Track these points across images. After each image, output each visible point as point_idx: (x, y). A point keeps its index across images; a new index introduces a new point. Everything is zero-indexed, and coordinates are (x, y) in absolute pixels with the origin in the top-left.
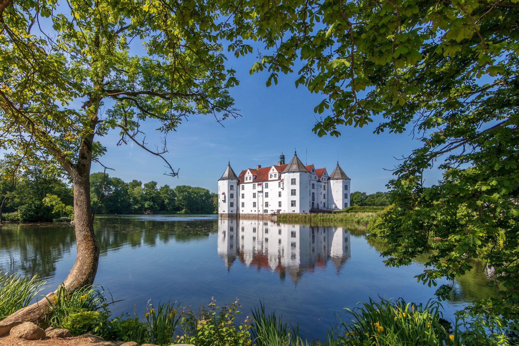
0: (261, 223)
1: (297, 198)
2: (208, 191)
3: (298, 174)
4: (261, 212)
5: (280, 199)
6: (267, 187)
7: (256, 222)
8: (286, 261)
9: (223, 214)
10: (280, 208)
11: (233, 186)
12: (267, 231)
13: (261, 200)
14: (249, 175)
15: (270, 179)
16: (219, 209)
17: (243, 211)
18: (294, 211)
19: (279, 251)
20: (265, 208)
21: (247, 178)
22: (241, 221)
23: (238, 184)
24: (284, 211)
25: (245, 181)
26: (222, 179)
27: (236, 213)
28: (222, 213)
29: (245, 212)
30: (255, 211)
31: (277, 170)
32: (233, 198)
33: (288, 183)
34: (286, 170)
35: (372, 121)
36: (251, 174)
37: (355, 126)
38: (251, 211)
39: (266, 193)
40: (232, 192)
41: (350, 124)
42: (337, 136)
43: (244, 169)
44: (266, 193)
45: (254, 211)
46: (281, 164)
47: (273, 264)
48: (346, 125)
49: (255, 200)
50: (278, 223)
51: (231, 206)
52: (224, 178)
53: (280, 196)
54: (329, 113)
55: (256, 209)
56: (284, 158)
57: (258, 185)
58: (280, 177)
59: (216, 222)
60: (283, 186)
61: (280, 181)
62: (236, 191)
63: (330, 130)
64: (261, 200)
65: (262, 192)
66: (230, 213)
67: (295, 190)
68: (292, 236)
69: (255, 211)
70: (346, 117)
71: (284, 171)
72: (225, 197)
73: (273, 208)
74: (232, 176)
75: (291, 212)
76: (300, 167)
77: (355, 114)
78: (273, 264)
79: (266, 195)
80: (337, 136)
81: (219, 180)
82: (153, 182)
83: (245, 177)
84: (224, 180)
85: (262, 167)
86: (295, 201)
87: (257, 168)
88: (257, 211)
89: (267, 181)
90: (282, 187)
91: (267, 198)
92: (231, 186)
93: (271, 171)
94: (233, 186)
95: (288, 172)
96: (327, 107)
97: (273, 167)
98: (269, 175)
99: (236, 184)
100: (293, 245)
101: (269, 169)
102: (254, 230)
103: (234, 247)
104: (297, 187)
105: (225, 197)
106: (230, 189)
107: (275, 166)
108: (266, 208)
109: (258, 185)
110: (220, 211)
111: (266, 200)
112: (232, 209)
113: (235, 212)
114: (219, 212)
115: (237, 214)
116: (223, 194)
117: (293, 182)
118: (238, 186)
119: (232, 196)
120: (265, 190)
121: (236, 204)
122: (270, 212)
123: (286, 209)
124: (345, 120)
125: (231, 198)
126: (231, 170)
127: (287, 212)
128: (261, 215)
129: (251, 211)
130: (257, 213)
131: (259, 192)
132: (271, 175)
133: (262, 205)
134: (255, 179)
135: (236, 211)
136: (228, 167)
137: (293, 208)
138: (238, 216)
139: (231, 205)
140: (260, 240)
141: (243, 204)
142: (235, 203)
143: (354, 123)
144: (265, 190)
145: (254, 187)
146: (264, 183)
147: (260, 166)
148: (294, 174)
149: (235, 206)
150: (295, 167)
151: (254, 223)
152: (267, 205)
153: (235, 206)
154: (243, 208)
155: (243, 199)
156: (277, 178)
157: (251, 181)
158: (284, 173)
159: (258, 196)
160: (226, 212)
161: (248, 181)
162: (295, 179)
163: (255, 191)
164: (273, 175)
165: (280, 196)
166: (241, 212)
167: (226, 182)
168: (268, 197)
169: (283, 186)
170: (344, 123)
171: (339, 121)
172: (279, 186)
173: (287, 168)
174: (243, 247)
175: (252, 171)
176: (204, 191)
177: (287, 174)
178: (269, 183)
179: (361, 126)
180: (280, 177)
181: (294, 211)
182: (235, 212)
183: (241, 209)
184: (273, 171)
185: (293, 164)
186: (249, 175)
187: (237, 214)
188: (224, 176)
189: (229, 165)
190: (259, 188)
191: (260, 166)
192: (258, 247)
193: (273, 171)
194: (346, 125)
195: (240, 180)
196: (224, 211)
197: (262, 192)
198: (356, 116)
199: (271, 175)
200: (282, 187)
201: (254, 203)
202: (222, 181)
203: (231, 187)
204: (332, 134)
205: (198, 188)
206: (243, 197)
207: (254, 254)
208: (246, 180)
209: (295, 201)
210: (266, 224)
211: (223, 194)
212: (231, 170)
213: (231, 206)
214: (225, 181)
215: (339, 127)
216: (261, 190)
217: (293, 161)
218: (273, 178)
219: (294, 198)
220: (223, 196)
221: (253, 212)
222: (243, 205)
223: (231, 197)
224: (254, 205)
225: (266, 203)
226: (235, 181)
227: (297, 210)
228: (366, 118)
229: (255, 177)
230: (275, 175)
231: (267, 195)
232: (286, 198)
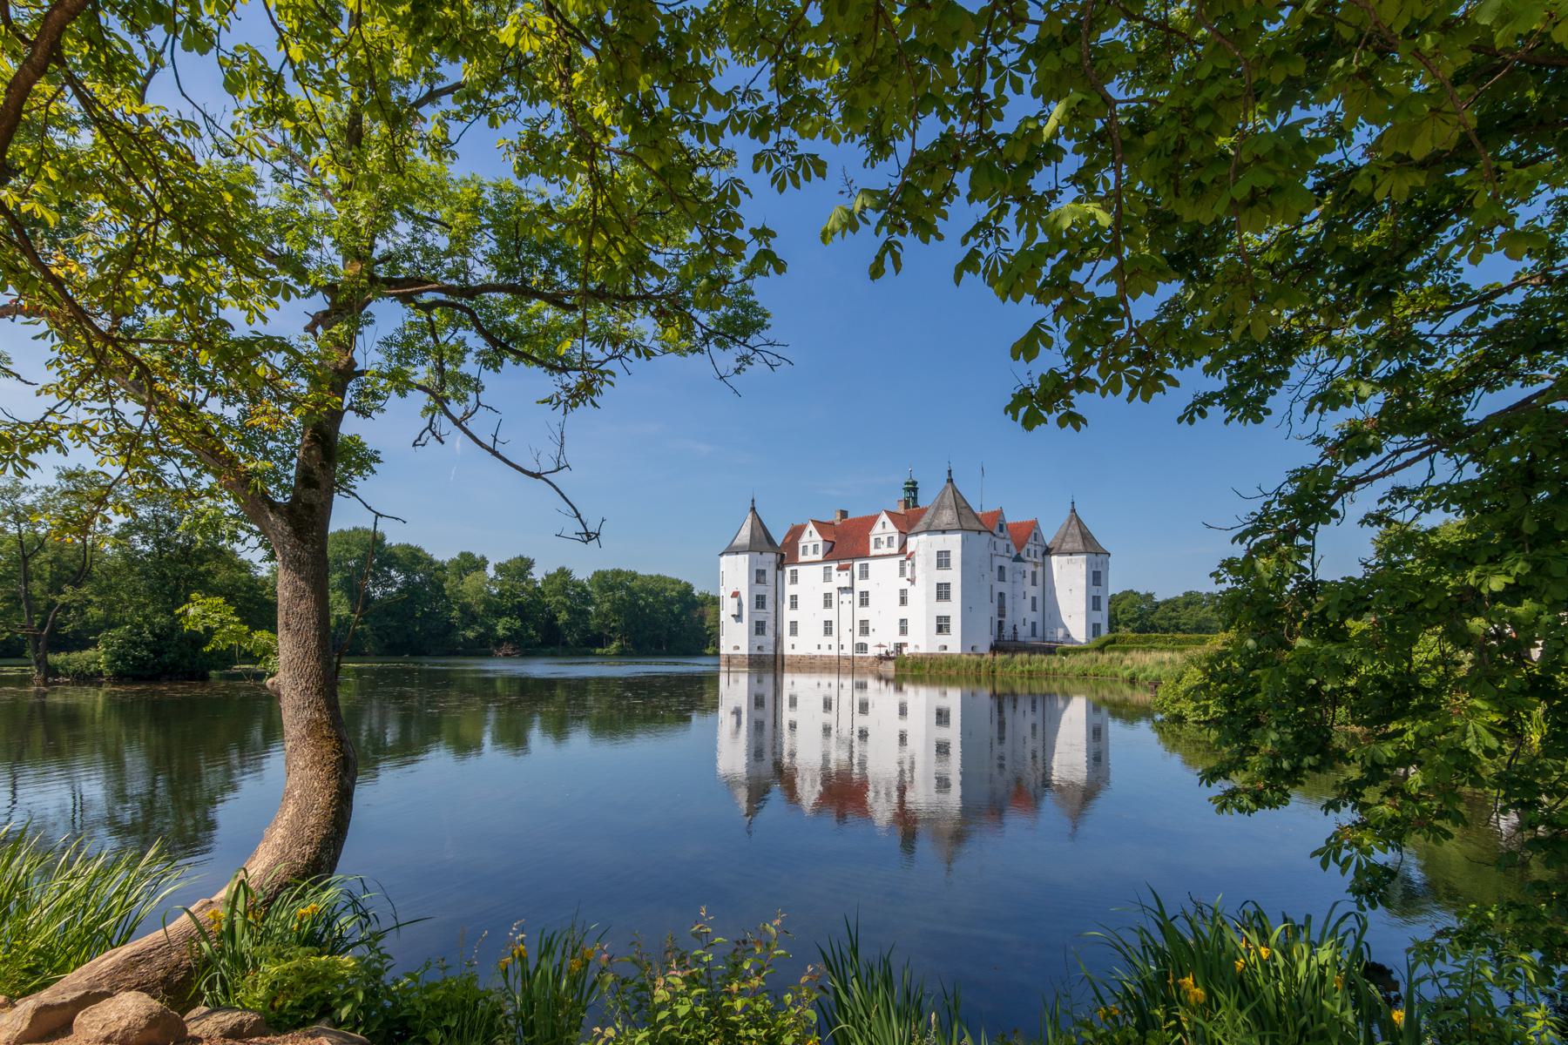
0: (848, 682)
2: (688, 589)
3: (958, 537)
5: (903, 612)
6: (865, 574)
7: (834, 680)
8: (921, 796)
9: (735, 656)
11: (763, 572)
12: (864, 707)
13: (846, 613)
14: (811, 539)
15: (873, 552)
16: (722, 642)
17: (793, 646)
18: (945, 648)
19: (902, 772)
20: (860, 639)
21: (805, 547)
22: (788, 678)
23: (780, 566)
24: (917, 647)
25: (801, 558)
26: (733, 550)
27: (772, 653)
28: (732, 652)
29: (798, 652)
30: (830, 647)
31: (896, 526)
32: (763, 607)
33: (928, 563)
34: (921, 525)
35: (1176, 384)
36: (817, 538)
37: (1130, 400)
38: (819, 647)
39: (862, 593)
40: (760, 590)
41: (1116, 391)
42: (1078, 429)
43: (797, 523)
44: (862, 593)
45: (826, 647)
46: (907, 506)
47: (882, 809)
48: (1103, 394)
49: (830, 614)
50: (898, 682)
51: (757, 633)
52: (737, 547)
53: (903, 601)
54: (1053, 359)
55: (832, 640)
56: (915, 490)
57: (839, 569)
58: (903, 545)
59: (714, 679)
60: (913, 572)
61: (903, 558)
62: (773, 588)
63: (1057, 411)
64: (846, 613)
65: (851, 589)
66: (755, 652)
67: (948, 585)
68: (939, 723)
69: (830, 647)
70: (1103, 372)
71: (916, 529)
72: (740, 605)
73: (883, 638)
74: (762, 540)
75: (935, 650)
76: (962, 517)
77: (1129, 363)
78: (882, 809)
79: (862, 601)
80: (1078, 429)
81: (722, 555)
82: (521, 558)
83: (801, 546)
84: (737, 553)
85: (851, 516)
86: (947, 618)
87: (836, 518)
88: (835, 647)
89: (866, 556)
90: (908, 575)
91: (864, 609)
92: (758, 571)
93: (877, 529)
94: (763, 572)
95: (929, 531)
96: (1048, 343)
97: (884, 517)
98: (872, 540)
99: (773, 566)
100: (942, 749)
101: (870, 521)
102: (827, 705)
103: (768, 758)
104: (953, 576)
105: (740, 605)
107: (889, 514)
108: (863, 639)
109: (839, 569)
110: (726, 648)
111: (862, 613)
112: (760, 640)
113: (769, 651)
114: (723, 651)
115: (776, 656)
116: (736, 595)
117: (943, 560)
118: (780, 572)
119: (760, 602)
120: (860, 586)
121: (773, 627)
122: (873, 652)
123: (921, 641)
124: (1100, 381)
125: (757, 607)
126: (759, 524)
127: (923, 650)
128: (846, 658)
129: (819, 647)
130: (834, 652)
131: (842, 590)
132: (877, 540)
133: (852, 630)
134: (831, 550)
135: (772, 647)
136: (750, 515)
137: (943, 639)
138: (779, 662)
139: (759, 628)
140: (845, 733)
141: (794, 625)
142: (770, 624)
143: (1126, 388)
144: (860, 586)
145: (827, 577)
146: (857, 564)
147: (844, 514)
148: (946, 536)
149: (770, 635)
150: (948, 516)
151: (826, 683)
152: (865, 628)
154: (793, 639)
155: (794, 611)
156: (895, 550)
157: (819, 557)
158: (917, 534)
159: (840, 603)
160: (744, 650)
161: (811, 557)
163: (831, 588)
164: (884, 538)
165: (903, 601)
166: (788, 651)
167: (743, 560)
168: (867, 604)
169: (913, 572)
170: (1098, 390)
171: (1083, 384)
172: (902, 572)
173: (926, 519)
174: (792, 755)
175: (821, 526)
176: (678, 588)
177: (923, 537)
178: (872, 563)
179: (1146, 398)
180: (903, 545)
181: (945, 648)
182: (769, 651)
183: (788, 640)
184: (884, 530)
185: (943, 508)
186: (811, 539)
187: (776, 656)
188: (737, 542)
189: (753, 509)
190: (842, 579)
191: (844, 514)
192: (838, 756)
193: (884, 530)
194: (1103, 394)
195: (786, 555)
196: (737, 648)
197: (851, 589)
198: (1133, 367)
199: (877, 540)
200: (908, 575)
201: (826, 622)
202: (733, 557)
203: (759, 576)
204: (1061, 423)
205: (660, 578)
206: (794, 605)
207: (826, 778)
208: (804, 553)
209: (947, 618)
210: (862, 686)
211: (736, 595)
212: (759, 524)
213: (757, 633)
215: (1082, 402)
216: (848, 585)
217: (942, 498)
218: (884, 550)
219: (945, 608)
221: (825, 652)
223: (757, 604)
224: (826, 629)
226: (771, 557)
227: (953, 643)
228: (1161, 375)
229: (830, 545)
230: (890, 539)
231: (864, 600)
232: (922, 609)
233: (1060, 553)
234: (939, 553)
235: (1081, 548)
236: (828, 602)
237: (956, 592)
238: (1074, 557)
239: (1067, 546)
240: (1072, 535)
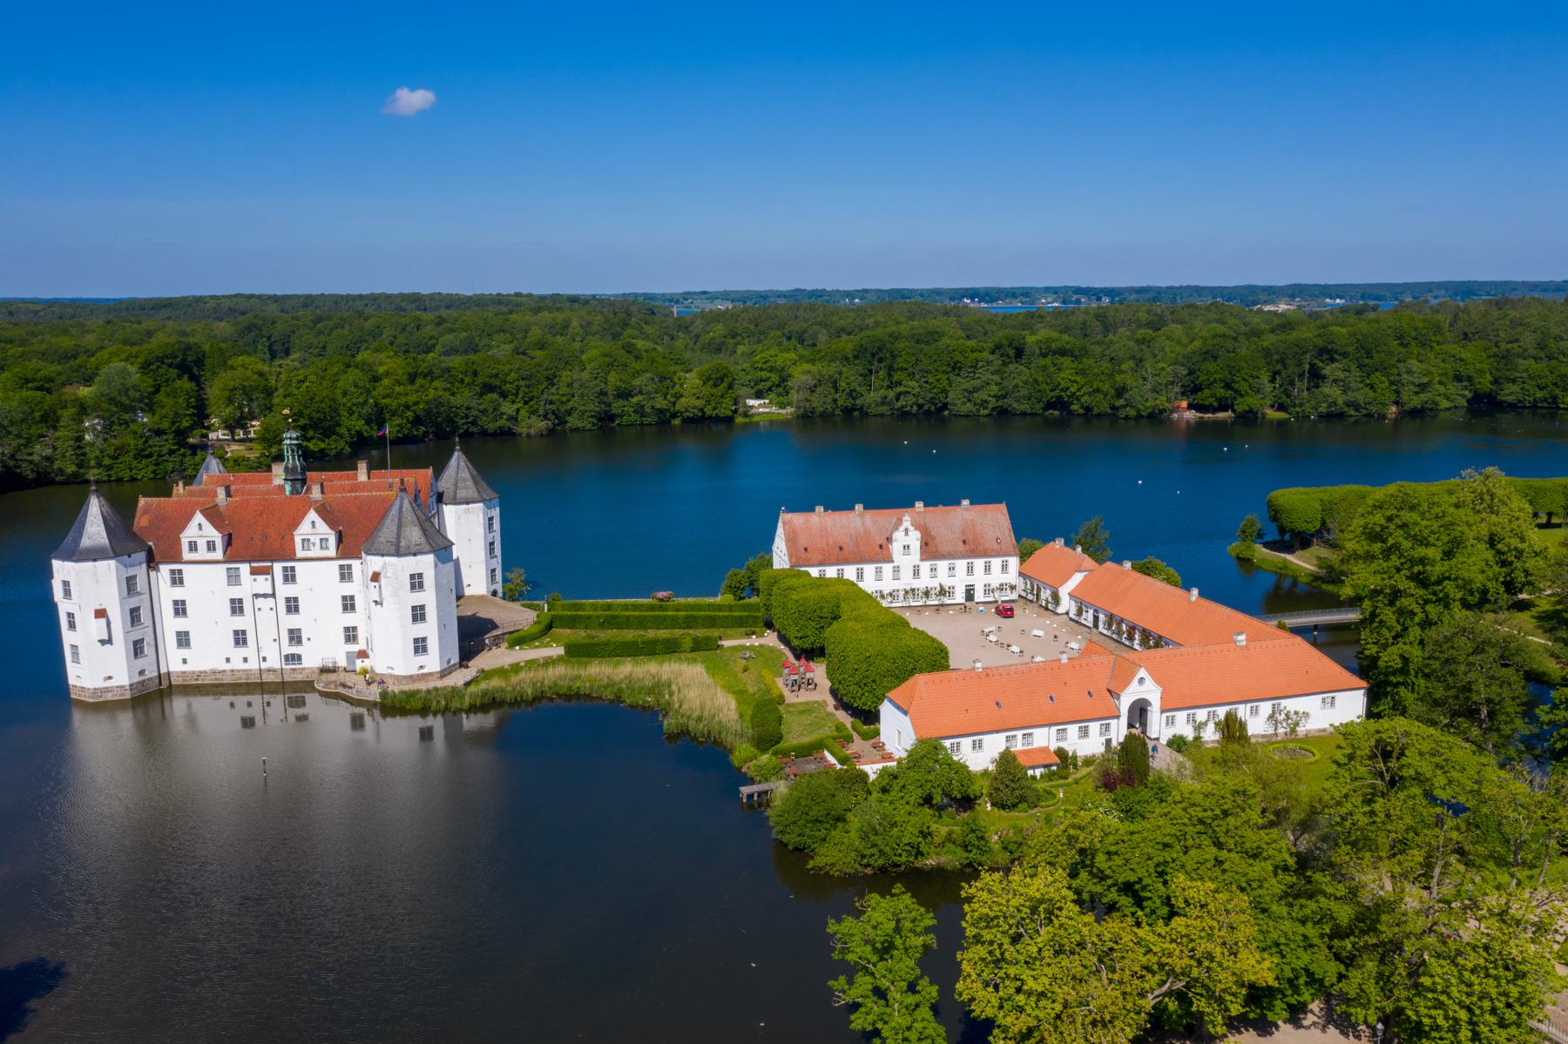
1: (429, 629)
3: (430, 558)
4: (274, 662)
5: (350, 619)
6: (290, 577)
10: (354, 648)
13: (267, 626)
15: (300, 553)
17: (185, 661)
23: (152, 562)
27: (156, 674)
28: (103, 684)
29: (196, 665)
30: (245, 660)
31: (331, 524)
38: (228, 660)
39: (288, 600)
44: (288, 600)
45: (243, 662)
49: (239, 623)
55: (249, 651)
66: (137, 679)
67: (422, 607)
69: (245, 660)
84: (95, 560)
86: (424, 640)
91: (293, 617)
98: (298, 540)
99: (144, 566)
106: (126, 592)
109: (254, 572)
111: (293, 621)
112: (141, 663)
113: (151, 673)
115: (160, 675)
116: (101, 613)
117: (416, 582)
118: (152, 574)
119: (134, 614)
121: (153, 643)
128: (269, 670)
129: (228, 660)
130: (253, 665)
137: (421, 659)
139: (137, 648)
144: (284, 591)
145: (234, 578)
146: (278, 567)
148: (420, 558)
152: (295, 636)
153: (148, 649)
154: (184, 653)
156: (332, 552)
162: (420, 575)
163: (236, 592)
164: (316, 539)
187: (160, 675)
190: (263, 584)
196: (110, 678)
197: (273, 595)
214: (102, 565)
216: (270, 592)
218: (316, 552)
219: (420, 630)
220: (103, 621)
221: (237, 664)
222: (183, 639)
225: (291, 631)
229: (227, 537)
231: (293, 606)
233: (456, 502)
234: (412, 576)
235: (476, 495)
236: (237, 607)
237: (431, 613)
238: (471, 506)
239: (462, 494)
240: (464, 480)
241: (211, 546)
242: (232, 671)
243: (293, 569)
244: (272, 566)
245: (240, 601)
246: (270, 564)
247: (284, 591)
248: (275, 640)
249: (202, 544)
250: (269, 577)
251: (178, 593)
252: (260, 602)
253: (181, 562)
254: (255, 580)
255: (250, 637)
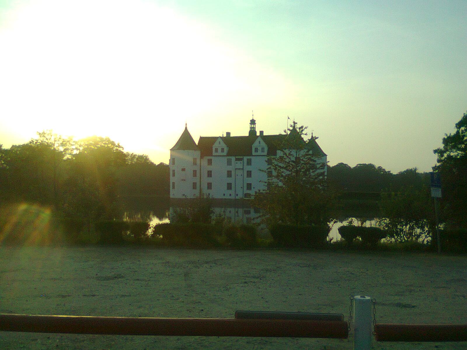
0: (241, 211)
4: (240, 196)
6: (249, 163)
15: (254, 153)
30: (230, 195)
38: (224, 195)
45: (229, 195)
49: (231, 180)
55: (232, 192)
69: (230, 195)
108: (248, 192)
109: (237, 160)
129: (224, 195)
130: (233, 197)
133: (242, 188)
144: (248, 168)
146: (245, 158)
152: (249, 186)
156: (265, 153)
157: (225, 153)
161: (220, 153)
163: (230, 168)
164: (260, 149)
190: (239, 165)
197: (243, 169)
218: (259, 153)
221: (227, 197)
222: (210, 186)
230: (263, 149)
231: (249, 174)
236: (229, 174)
241: (223, 150)
242: (225, 199)
243: (251, 159)
244: (243, 158)
245: (231, 171)
246: (242, 157)
247: (248, 168)
248: (242, 188)
249: (220, 150)
250: (242, 162)
251: (210, 168)
252: (237, 171)
253: (212, 156)
254: (237, 163)
255: (233, 186)
